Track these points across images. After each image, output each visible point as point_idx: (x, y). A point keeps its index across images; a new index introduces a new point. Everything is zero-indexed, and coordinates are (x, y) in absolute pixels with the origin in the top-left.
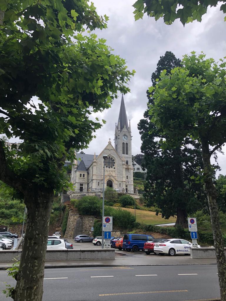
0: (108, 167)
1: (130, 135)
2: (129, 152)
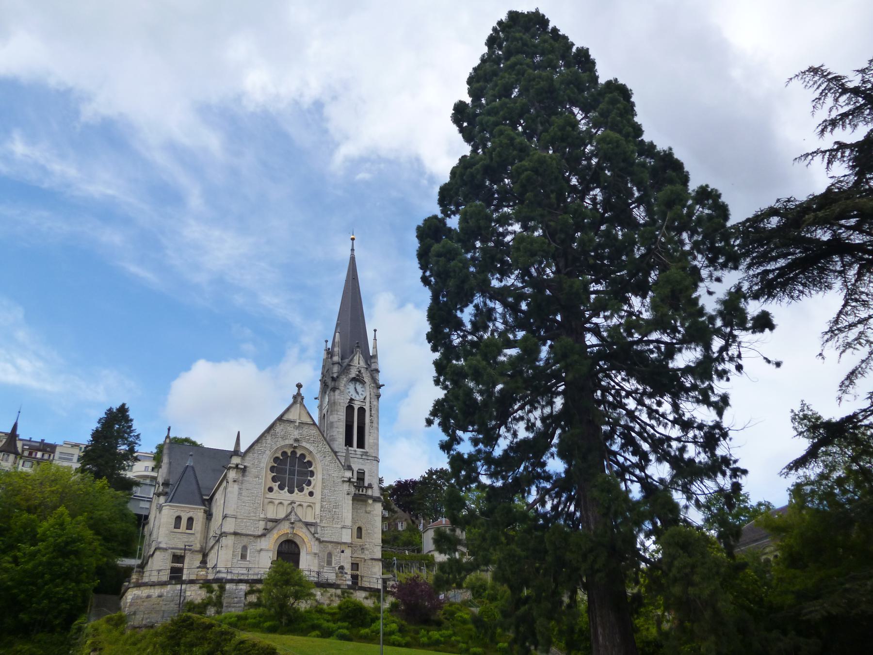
0: (286, 489)
1: (374, 380)
2: (368, 440)
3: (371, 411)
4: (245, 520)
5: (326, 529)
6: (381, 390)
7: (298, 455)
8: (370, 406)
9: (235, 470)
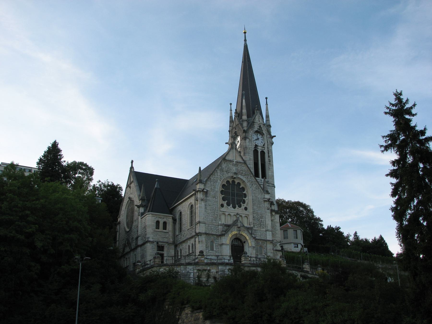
1: (269, 132)
2: (268, 173)
3: (268, 153)
4: (210, 225)
5: (257, 231)
6: (274, 140)
7: (236, 183)
8: (268, 150)
9: (202, 193)
